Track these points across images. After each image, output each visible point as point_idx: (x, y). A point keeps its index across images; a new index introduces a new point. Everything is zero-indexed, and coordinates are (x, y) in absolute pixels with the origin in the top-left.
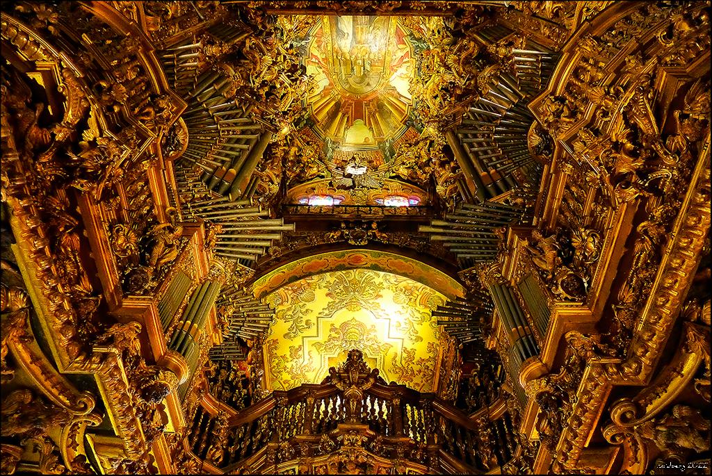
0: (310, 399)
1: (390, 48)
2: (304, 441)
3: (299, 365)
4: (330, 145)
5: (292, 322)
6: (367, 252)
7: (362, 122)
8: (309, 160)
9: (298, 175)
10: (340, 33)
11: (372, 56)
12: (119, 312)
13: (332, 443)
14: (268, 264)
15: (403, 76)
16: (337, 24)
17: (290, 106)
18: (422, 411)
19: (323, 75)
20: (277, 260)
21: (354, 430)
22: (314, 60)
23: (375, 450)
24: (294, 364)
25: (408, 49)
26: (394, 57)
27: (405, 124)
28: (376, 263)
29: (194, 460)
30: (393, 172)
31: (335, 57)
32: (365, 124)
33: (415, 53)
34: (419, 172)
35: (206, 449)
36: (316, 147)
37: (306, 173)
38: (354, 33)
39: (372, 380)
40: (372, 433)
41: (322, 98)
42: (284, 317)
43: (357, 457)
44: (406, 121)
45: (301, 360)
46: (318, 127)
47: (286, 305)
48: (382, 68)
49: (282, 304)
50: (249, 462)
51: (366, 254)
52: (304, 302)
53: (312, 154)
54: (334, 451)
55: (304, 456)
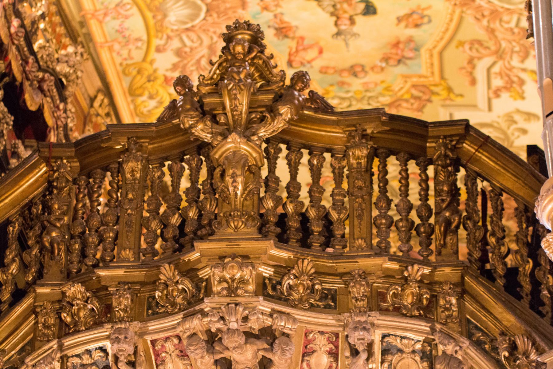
0: (131, 164)
2: (121, 283)
13: (187, 285)
18: (431, 170)
21: (234, 256)
23: (296, 296)
39: (285, 111)
40: (284, 254)
43: (245, 319)
55: (121, 320)
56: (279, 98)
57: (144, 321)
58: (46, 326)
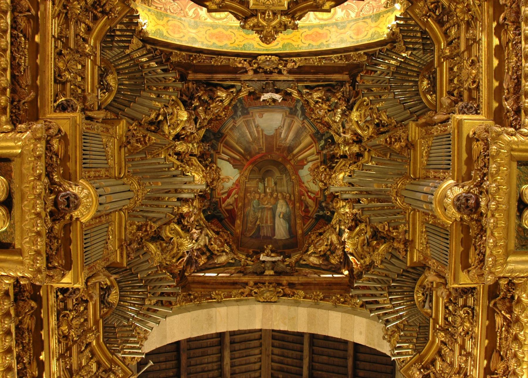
1: (240, 205)
4: (299, 112)
6: (259, 50)
7: (265, 133)
8: (320, 104)
10: (287, 218)
11: (257, 196)
15: (227, 180)
16: (290, 227)
17: (337, 162)
22: (312, 196)
25: (223, 205)
26: (236, 196)
27: (222, 134)
28: (247, 36)
30: (232, 92)
32: (262, 131)
33: (216, 203)
34: (205, 98)
37: (324, 95)
38: (274, 217)
41: (305, 158)
44: (221, 137)
48: (247, 185)
51: (259, 47)
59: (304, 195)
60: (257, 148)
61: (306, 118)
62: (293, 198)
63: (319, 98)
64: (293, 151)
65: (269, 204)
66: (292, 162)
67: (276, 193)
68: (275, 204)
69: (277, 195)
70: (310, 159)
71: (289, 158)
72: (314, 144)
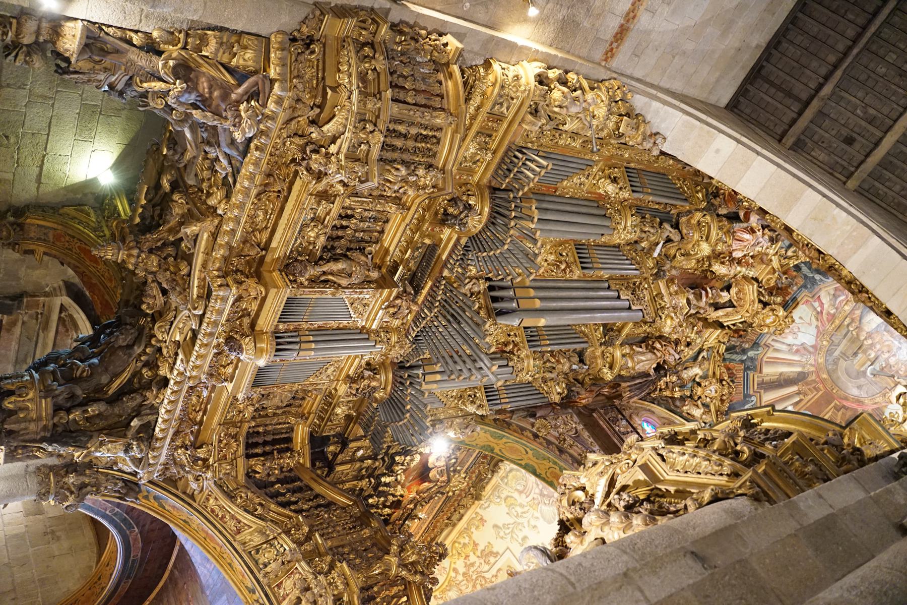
2: (317, 543)
3: (479, 570)
5: (512, 522)
9: (672, 398)
11: (892, 361)
12: (266, 275)
13: (326, 568)
14: (523, 429)
17: (734, 325)
19: (814, 331)
20: (536, 436)
21: (345, 579)
22: (816, 304)
24: (477, 564)
29: (238, 445)
31: (846, 323)
35: (257, 455)
36: (726, 391)
37: (684, 405)
39: (418, 578)
42: (510, 506)
43: (321, 596)
45: (486, 568)
46: (755, 378)
47: (522, 499)
49: (521, 492)
50: (273, 506)
52: (539, 515)
53: (713, 394)
54: (317, 573)
56: (422, 573)
57: (304, 558)
58: (286, 526)
59: (828, 314)
60: (840, 413)
61: (747, 396)
62: (848, 321)
63: (697, 406)
64: (800, 373)
65: (885, 338)
66: (812, 361)
67: (865, 342)
68: (877, 332)
69: (866, 339)
70: (784, 347)
71: (813, 369)
72: (765, 359)
